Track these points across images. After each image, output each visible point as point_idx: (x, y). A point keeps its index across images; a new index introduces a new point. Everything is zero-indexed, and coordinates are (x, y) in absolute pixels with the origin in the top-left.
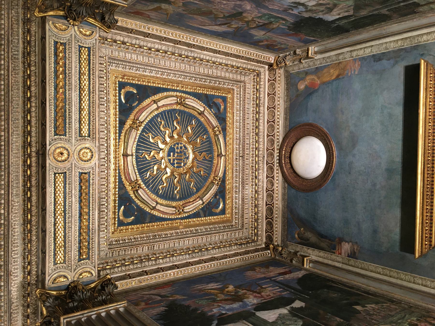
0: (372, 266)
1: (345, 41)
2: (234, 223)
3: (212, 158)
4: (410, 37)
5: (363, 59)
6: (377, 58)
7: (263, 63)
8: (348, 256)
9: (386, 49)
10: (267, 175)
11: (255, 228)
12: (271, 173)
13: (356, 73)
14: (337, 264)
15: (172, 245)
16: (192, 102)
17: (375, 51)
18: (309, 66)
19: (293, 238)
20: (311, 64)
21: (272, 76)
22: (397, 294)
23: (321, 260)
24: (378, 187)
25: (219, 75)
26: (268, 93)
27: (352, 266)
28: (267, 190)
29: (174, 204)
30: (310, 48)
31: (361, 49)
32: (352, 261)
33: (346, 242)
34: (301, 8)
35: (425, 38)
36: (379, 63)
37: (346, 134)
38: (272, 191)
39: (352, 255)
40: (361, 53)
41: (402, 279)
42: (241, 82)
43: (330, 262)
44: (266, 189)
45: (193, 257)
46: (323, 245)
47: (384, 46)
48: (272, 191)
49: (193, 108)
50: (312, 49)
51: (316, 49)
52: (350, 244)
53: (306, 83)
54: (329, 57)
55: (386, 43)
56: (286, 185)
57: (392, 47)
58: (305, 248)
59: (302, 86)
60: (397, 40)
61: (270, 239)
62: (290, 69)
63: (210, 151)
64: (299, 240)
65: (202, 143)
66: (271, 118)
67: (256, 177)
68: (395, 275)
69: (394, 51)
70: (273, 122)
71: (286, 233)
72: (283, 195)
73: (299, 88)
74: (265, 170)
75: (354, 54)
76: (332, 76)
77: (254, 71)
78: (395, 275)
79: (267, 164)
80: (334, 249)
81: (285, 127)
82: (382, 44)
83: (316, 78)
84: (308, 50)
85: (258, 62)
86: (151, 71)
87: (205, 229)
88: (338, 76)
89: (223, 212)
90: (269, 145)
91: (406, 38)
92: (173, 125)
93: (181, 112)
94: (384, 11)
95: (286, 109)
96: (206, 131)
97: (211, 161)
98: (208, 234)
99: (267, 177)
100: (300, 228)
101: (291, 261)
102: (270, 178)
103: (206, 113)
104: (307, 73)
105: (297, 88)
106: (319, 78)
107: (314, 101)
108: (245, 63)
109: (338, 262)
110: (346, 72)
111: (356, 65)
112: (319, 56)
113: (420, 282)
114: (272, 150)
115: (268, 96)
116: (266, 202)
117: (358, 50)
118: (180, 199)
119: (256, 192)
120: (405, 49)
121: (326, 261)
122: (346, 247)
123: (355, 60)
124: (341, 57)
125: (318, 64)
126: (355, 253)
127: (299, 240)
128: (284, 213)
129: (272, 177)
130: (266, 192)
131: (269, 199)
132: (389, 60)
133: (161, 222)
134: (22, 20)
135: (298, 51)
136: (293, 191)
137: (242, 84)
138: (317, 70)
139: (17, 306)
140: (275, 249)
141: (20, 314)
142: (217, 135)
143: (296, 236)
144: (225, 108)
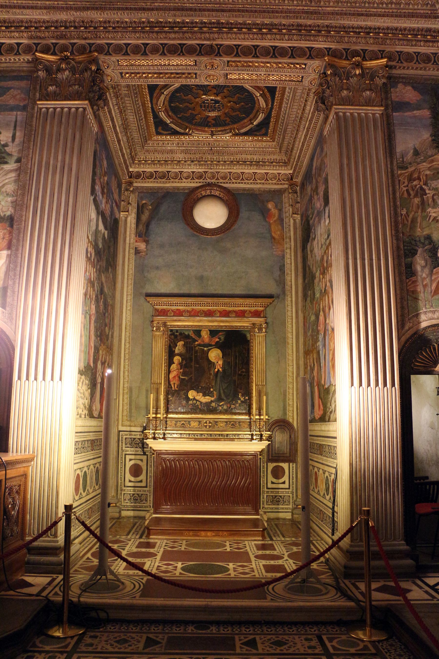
0: (132, 266)
1: (299, 245)
2: (149, 142)
3: (209, 127)
4: (292, 290)
5: (283, 257)
6: (282, 269)
7: (294, 171)
8: (136, 248)
9: (287, 274)
10: (194, 172)
11: (145, 161)
12: (196, 176)
13: (274, 253)
14: (128, 239)
15: (129, 108)
16: (261, 117)
17: (287, 266)
18: (286, 213)
19: (142, 199)
20: (287, 214)
21: (283, 177)
22: (119, 285)
23: (128, 225)
24: (191, 270)
25: (286, 137)
26: (268, 173)
27: (129, 251)
28: (181, 172)
29: (166, 103)
30: (299, 216)
31: (291, 256)
32: (132, 251)
33: (146, 246)
34: (314, 237)
35: (290, 299)
36: (278, 269)
37: (229, 245)
38: (181, 178)
39: (137, 252)
40: (288, 256)
41: (127, 287)
42: (280, 149)
43: (128, 233)
44: (182, 172)
45: (119, 127)
46: (141, 227)
47: (290, 273)
48: (181, 178)
49: (256, 117)
50: (298, 217)
51: (297, 221)
52: (145, 250)
53: (273, 210)
54: (290, 230)
55: (291, 274)
56: (186, 191)
57: (288, 278)
58: (135, 210)
59: (270, 206)
60: (291, 282)
61: (138, 176)
62: (286, 194)
63: (216, 125)
64: (141, 205)
65: (225, 121)
66: (246, 177)
67: (192, 161)
68: (130, 282)
69: (284, 279)
70: (242, 178)
71: (145, 191)
72: (178, 188)
73: (269, 203)
74: (200, 170)
75: (288, 251)
76: (275, 233)
77: (289, 160)
78: (130, 282)
79: (204, 172)
80: (140, 236)
81: (238, 189)
82: (291, 271)
83: (275, 219)
84: (298, 214)
85: (297, 165)
86: (290, 93)
87: (143, 125)
88: (274, 238)
89: (158, 133)
90: (222, 175)
91: (292, 287)
92: (240, 103)
93: (252, 108)
94: (306, 281)
95: (252, 189)
96: (234, 123)
97: (207, 126)
98: (139, 128)
99: (193, 172)
100: (151, 205)
101: (123, 201)
102: (192, 176)
103: (251, 126)
104: (280, 210)
105: (270, 201)
106: (275, 221)
107: (257, 217)
108: (295, 158)
109: (130, 240)
110: (275, 244)
111: (280, 253)
112: (292, 221)
113: (129, 298)
114: (218, 178)
115: (266, 173)
116: (170, 172)
117: (291, 253)
118: (170, 106)
119: (179, 161)
120: (284, 287)
121: (128, 230)
122: (142, 246)
123: (283, 251)
124: (288, 240)
125: (286, 220)
126: (139, 253)
127: (141, 205)
128: (162, 189)
129: (193, 177)
130: (180, 172)
131: (173, 175)
132: (279, 276)
133: (149, 95)
134: (331, 23)
135: (298, 205)
136: (182, 198)
137: (278, 150)
138: (281, 220)
139: (73, 15)
140: (131, 183)
141: (66, 17)
142: (231, 132)
143: (144, 202)
144: (256, 135)
